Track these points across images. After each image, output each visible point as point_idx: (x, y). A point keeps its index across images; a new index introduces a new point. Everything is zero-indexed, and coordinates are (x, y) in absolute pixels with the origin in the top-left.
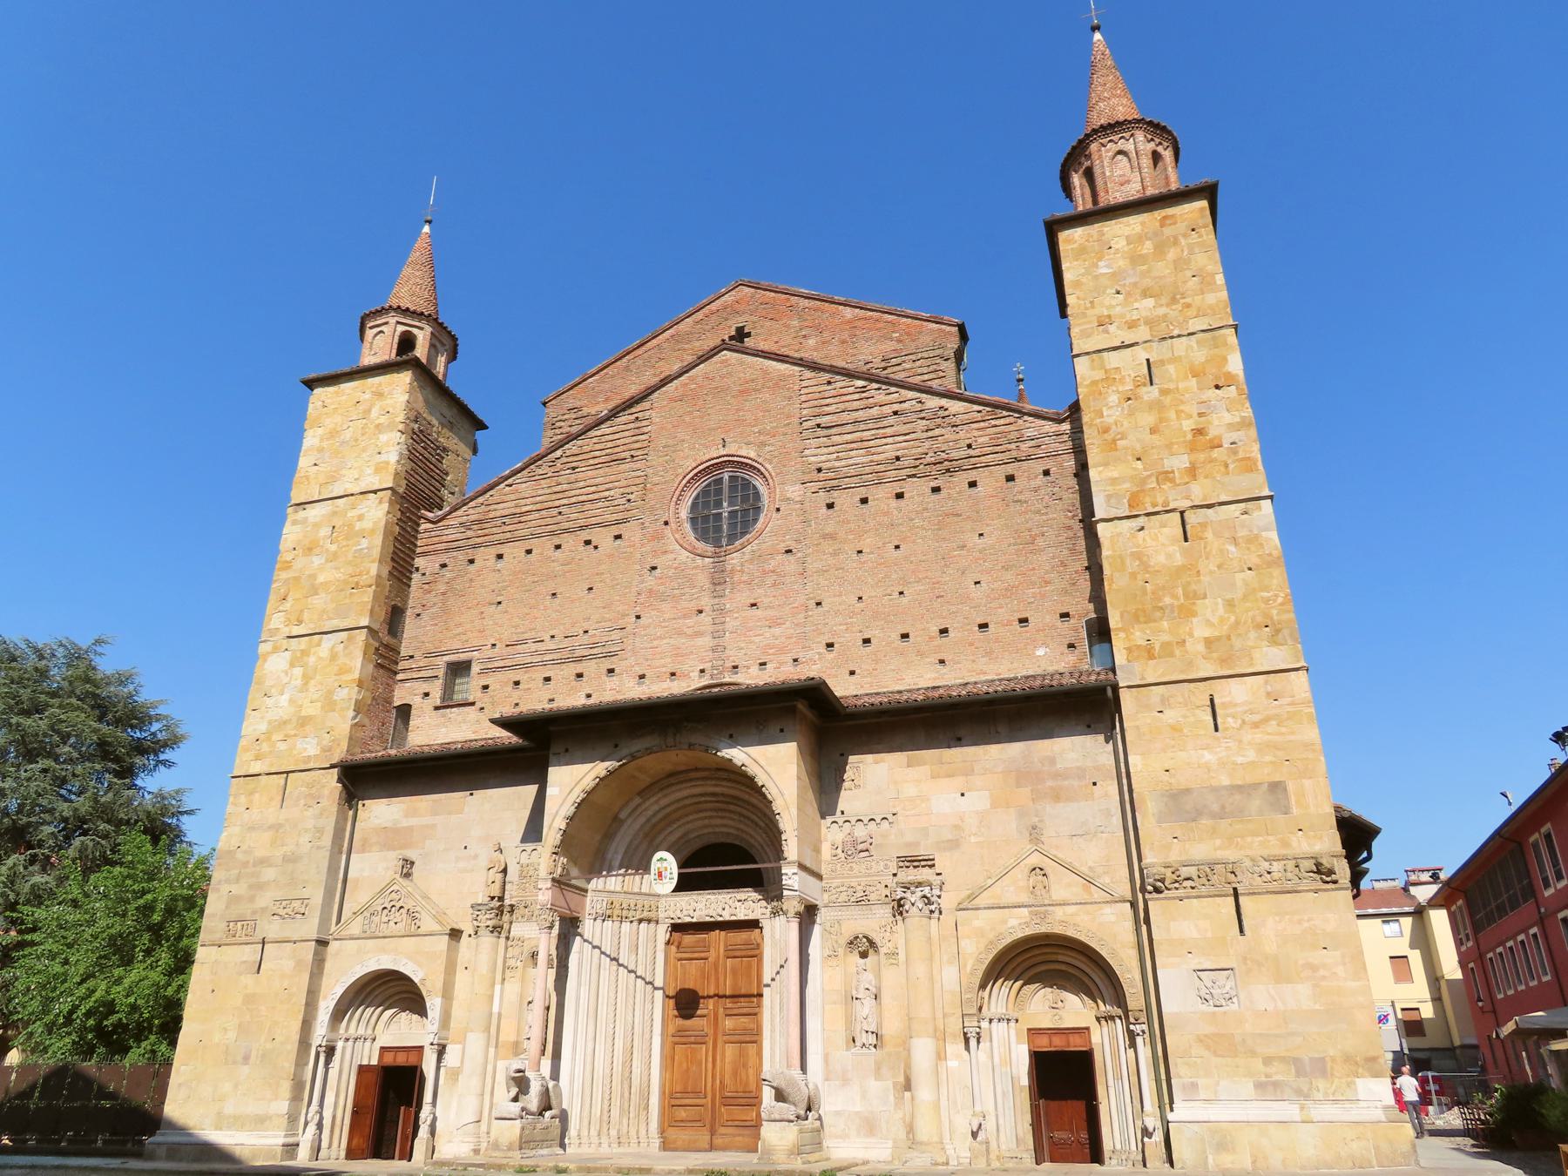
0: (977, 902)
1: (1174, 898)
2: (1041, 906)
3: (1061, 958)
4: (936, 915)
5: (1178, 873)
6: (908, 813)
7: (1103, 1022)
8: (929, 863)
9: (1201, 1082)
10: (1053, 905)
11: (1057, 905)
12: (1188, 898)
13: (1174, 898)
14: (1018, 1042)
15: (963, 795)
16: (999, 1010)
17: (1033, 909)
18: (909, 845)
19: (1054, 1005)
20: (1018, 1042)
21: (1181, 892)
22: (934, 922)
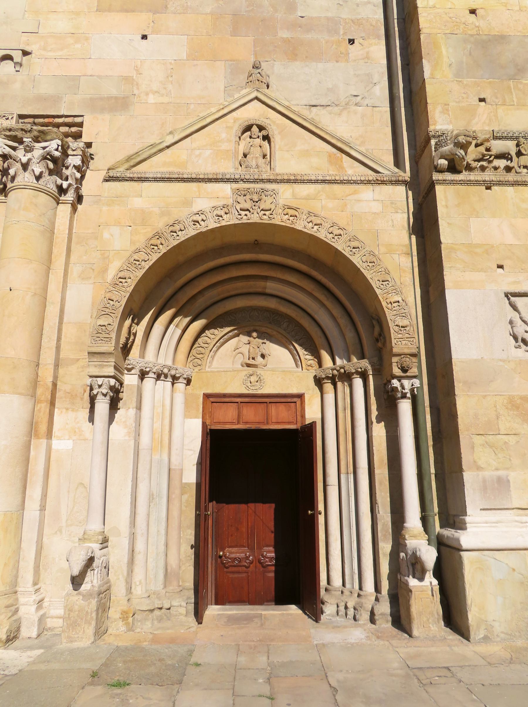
0: (143, 169)
1: (477, 183)
2: (255, 181)
3: (271, 287)
4: (70, 196)
5: (487, 144)
6: (50, 54)
7: (328, 387)
8: (74, 129)
9: (513, 476)
10: (275, 181)
11: (282, 181)
12: (500, 183)
13: (477, 183)
14: (187, 415)
15: (144, 37)
16: (161, 361)
17: (242, 185)
18: (41, 99)
19: (251, 362)
20: (187, 415)
21: (488, 176)
22: (64, 210)
